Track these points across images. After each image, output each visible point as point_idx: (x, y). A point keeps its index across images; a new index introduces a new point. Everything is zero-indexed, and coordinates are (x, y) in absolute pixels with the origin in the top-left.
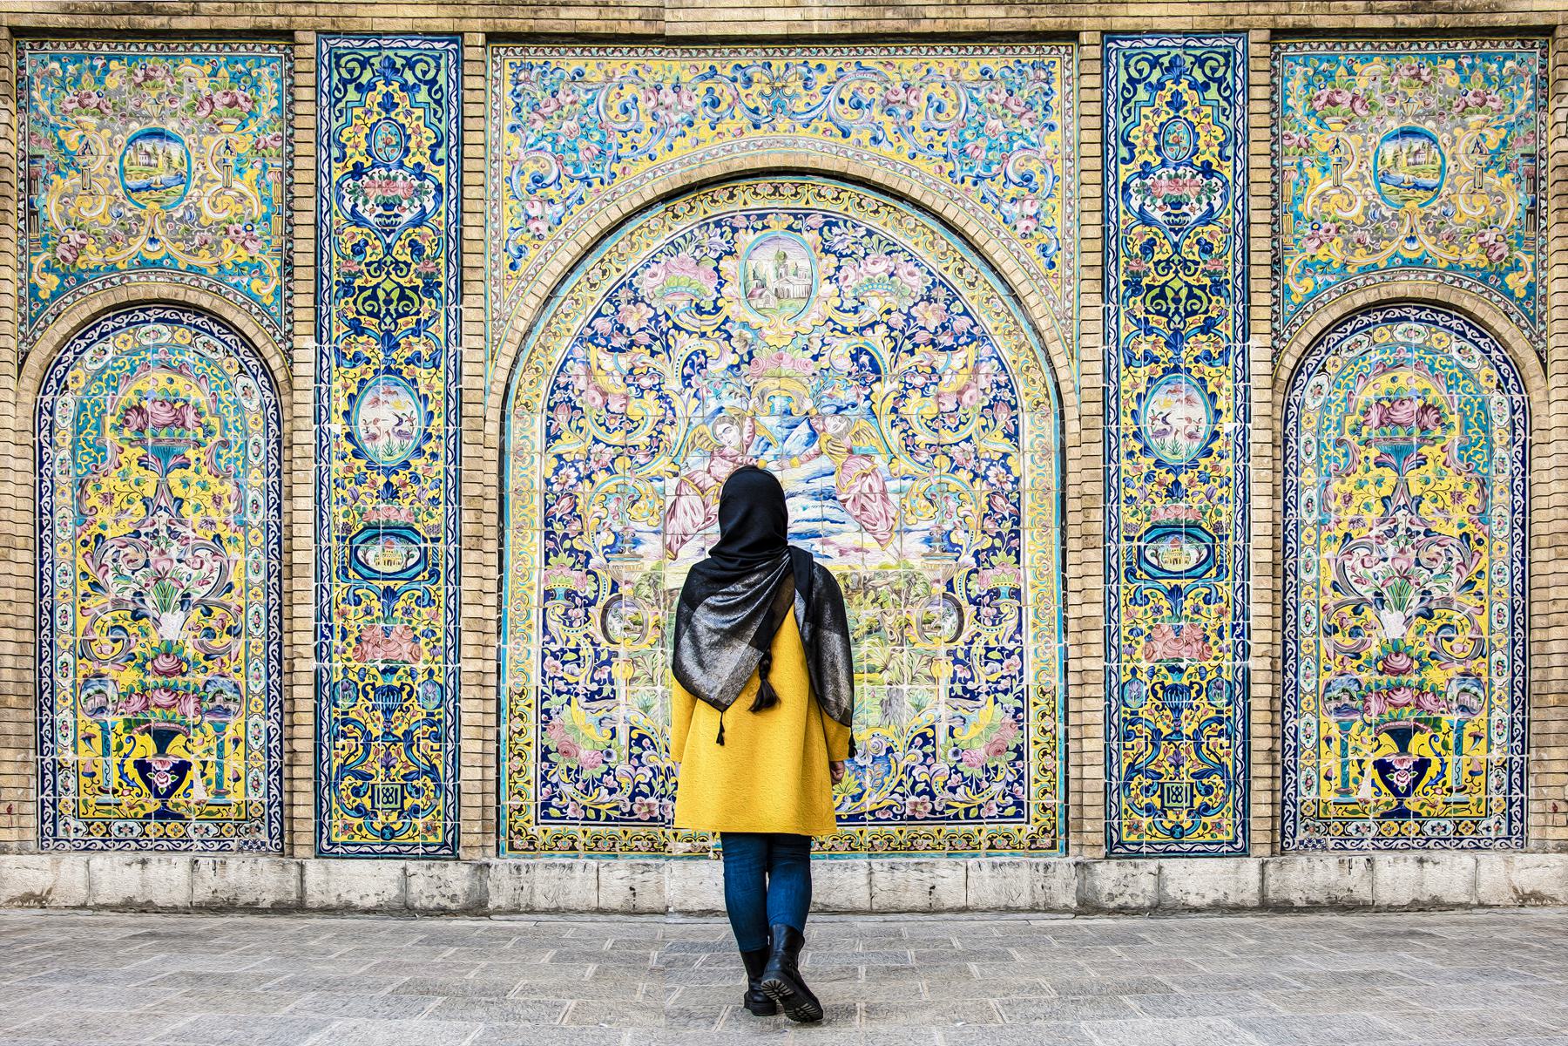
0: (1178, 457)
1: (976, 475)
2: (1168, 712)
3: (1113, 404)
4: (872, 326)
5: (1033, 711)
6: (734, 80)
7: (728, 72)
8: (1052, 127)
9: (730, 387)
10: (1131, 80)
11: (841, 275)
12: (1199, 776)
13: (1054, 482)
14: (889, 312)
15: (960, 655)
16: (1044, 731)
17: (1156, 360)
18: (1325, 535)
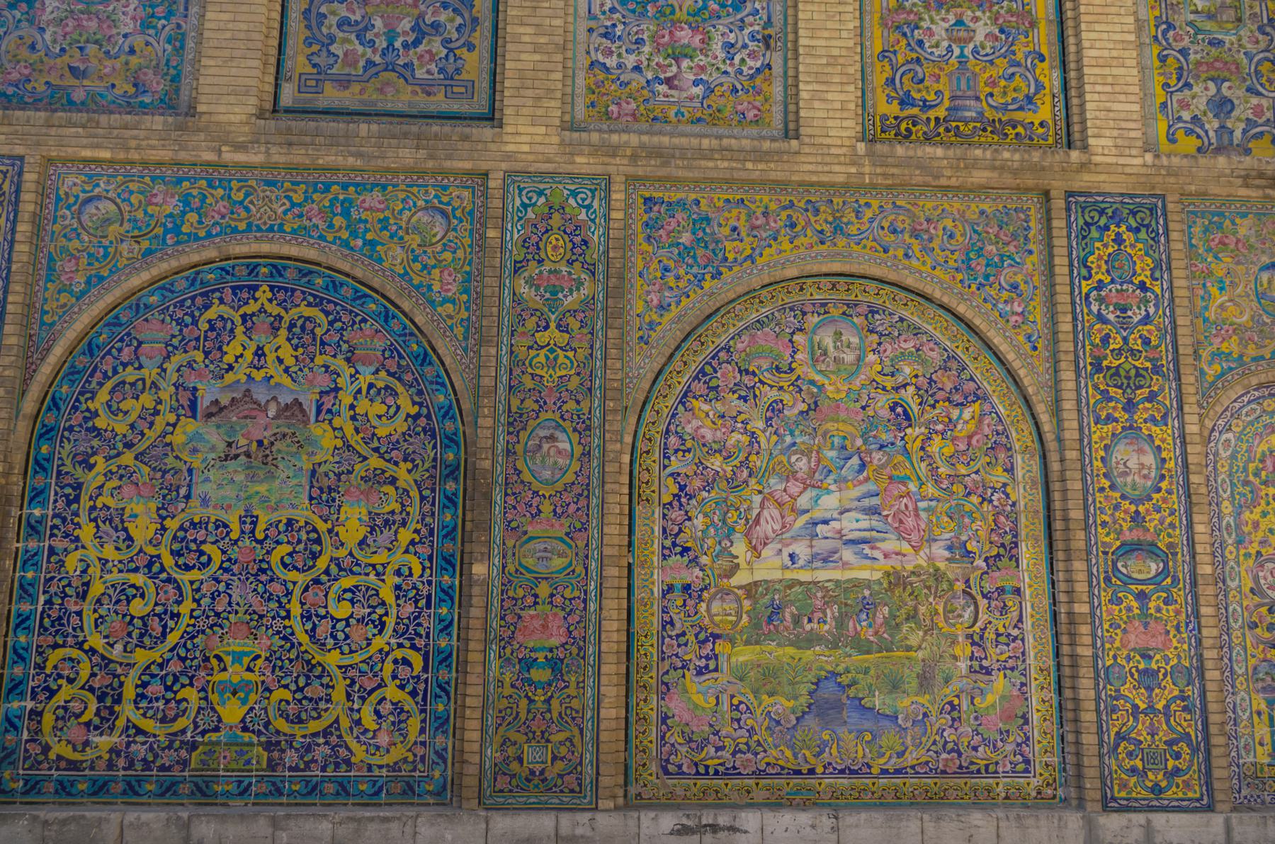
0: (1137, 493)
1: (984, 500)
2: (1143, 691)
3: (1087, 451)
4: (904, 386)
5: (1034, 684)
6: (807, 210)
7: (802, 204)
8: (1031, 252)
9: (801, 427)
10: (1086, 223)
11: (881, 349)
12: (1170, 743)
13: (1041, 506)
14: (916, 376)
15: (976, 638)
16: (1043, 701)
17: (1116, 420)
18: (1242, 552)
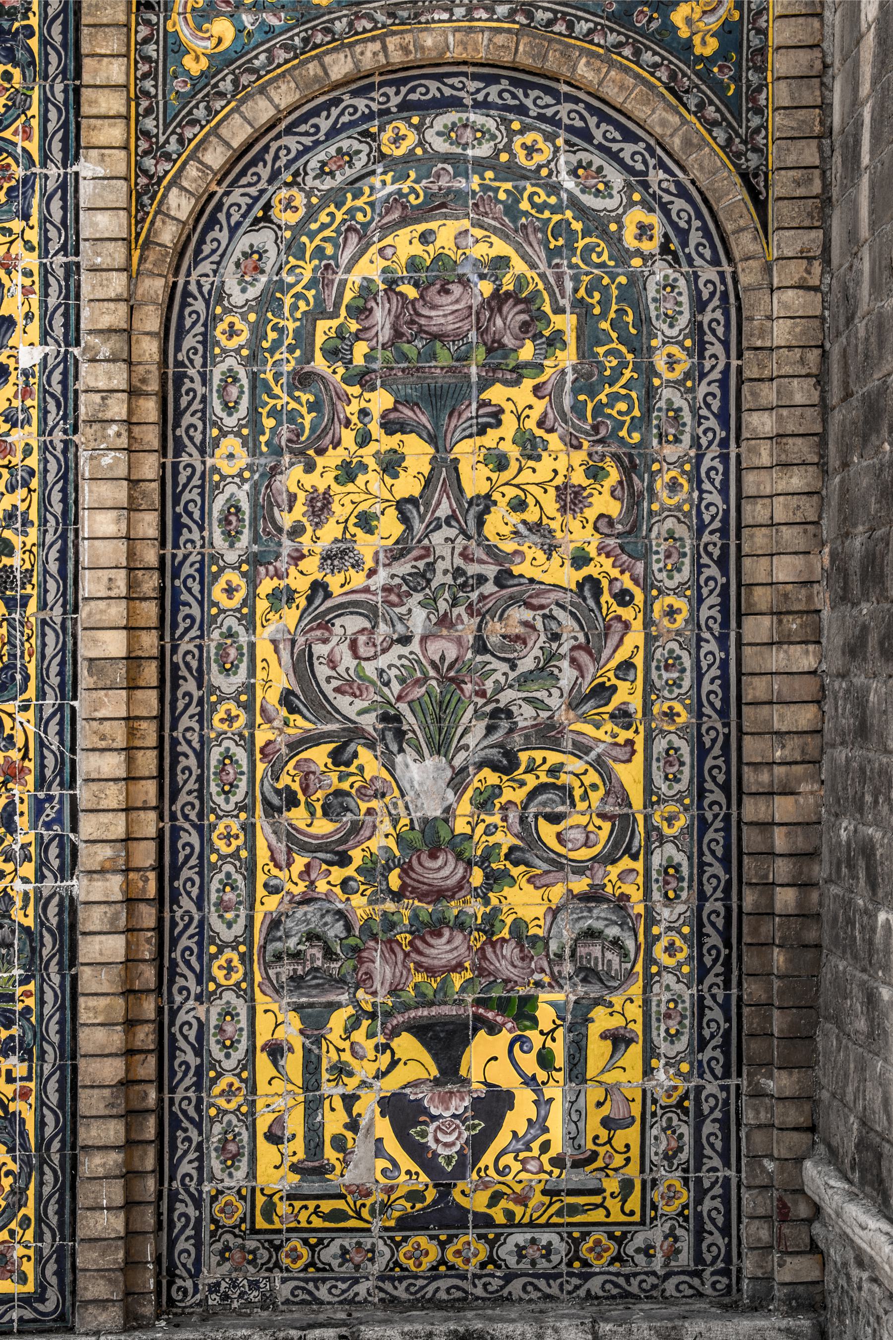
18: (267, 586)
